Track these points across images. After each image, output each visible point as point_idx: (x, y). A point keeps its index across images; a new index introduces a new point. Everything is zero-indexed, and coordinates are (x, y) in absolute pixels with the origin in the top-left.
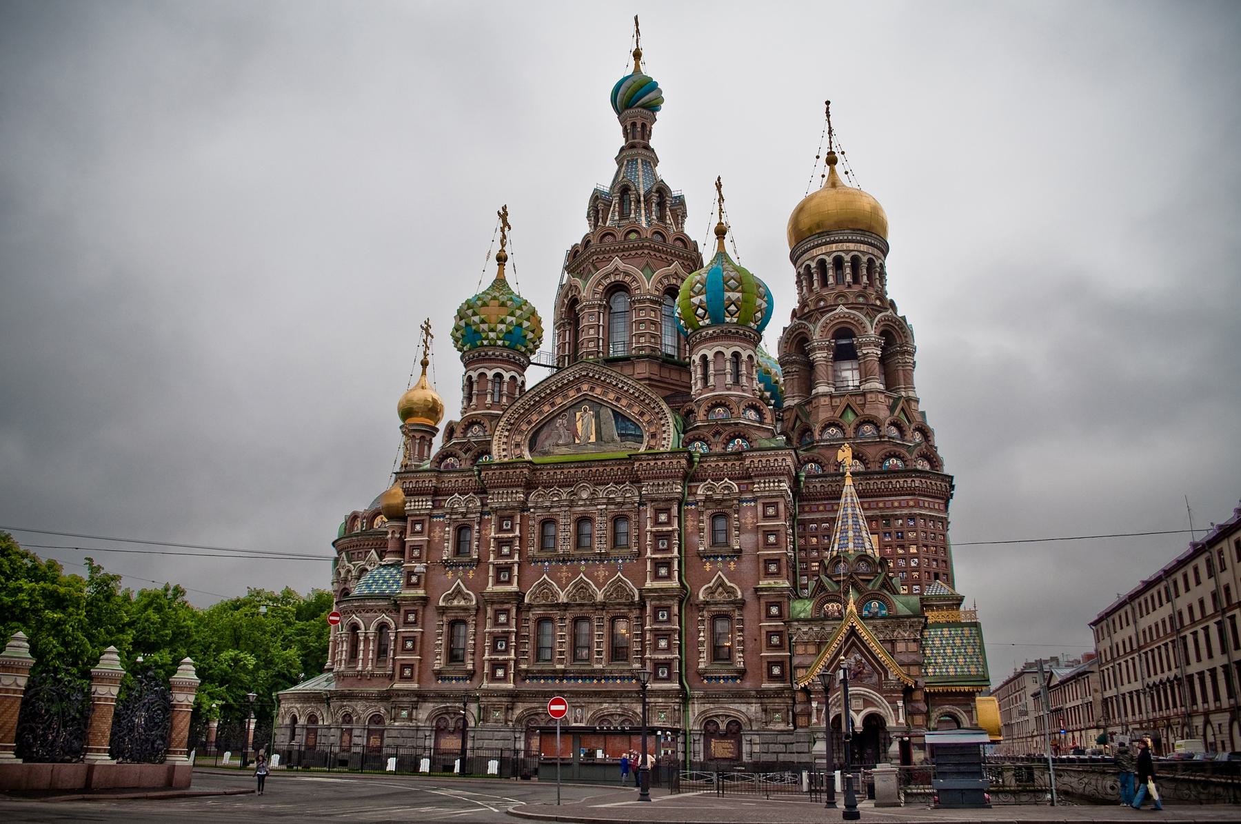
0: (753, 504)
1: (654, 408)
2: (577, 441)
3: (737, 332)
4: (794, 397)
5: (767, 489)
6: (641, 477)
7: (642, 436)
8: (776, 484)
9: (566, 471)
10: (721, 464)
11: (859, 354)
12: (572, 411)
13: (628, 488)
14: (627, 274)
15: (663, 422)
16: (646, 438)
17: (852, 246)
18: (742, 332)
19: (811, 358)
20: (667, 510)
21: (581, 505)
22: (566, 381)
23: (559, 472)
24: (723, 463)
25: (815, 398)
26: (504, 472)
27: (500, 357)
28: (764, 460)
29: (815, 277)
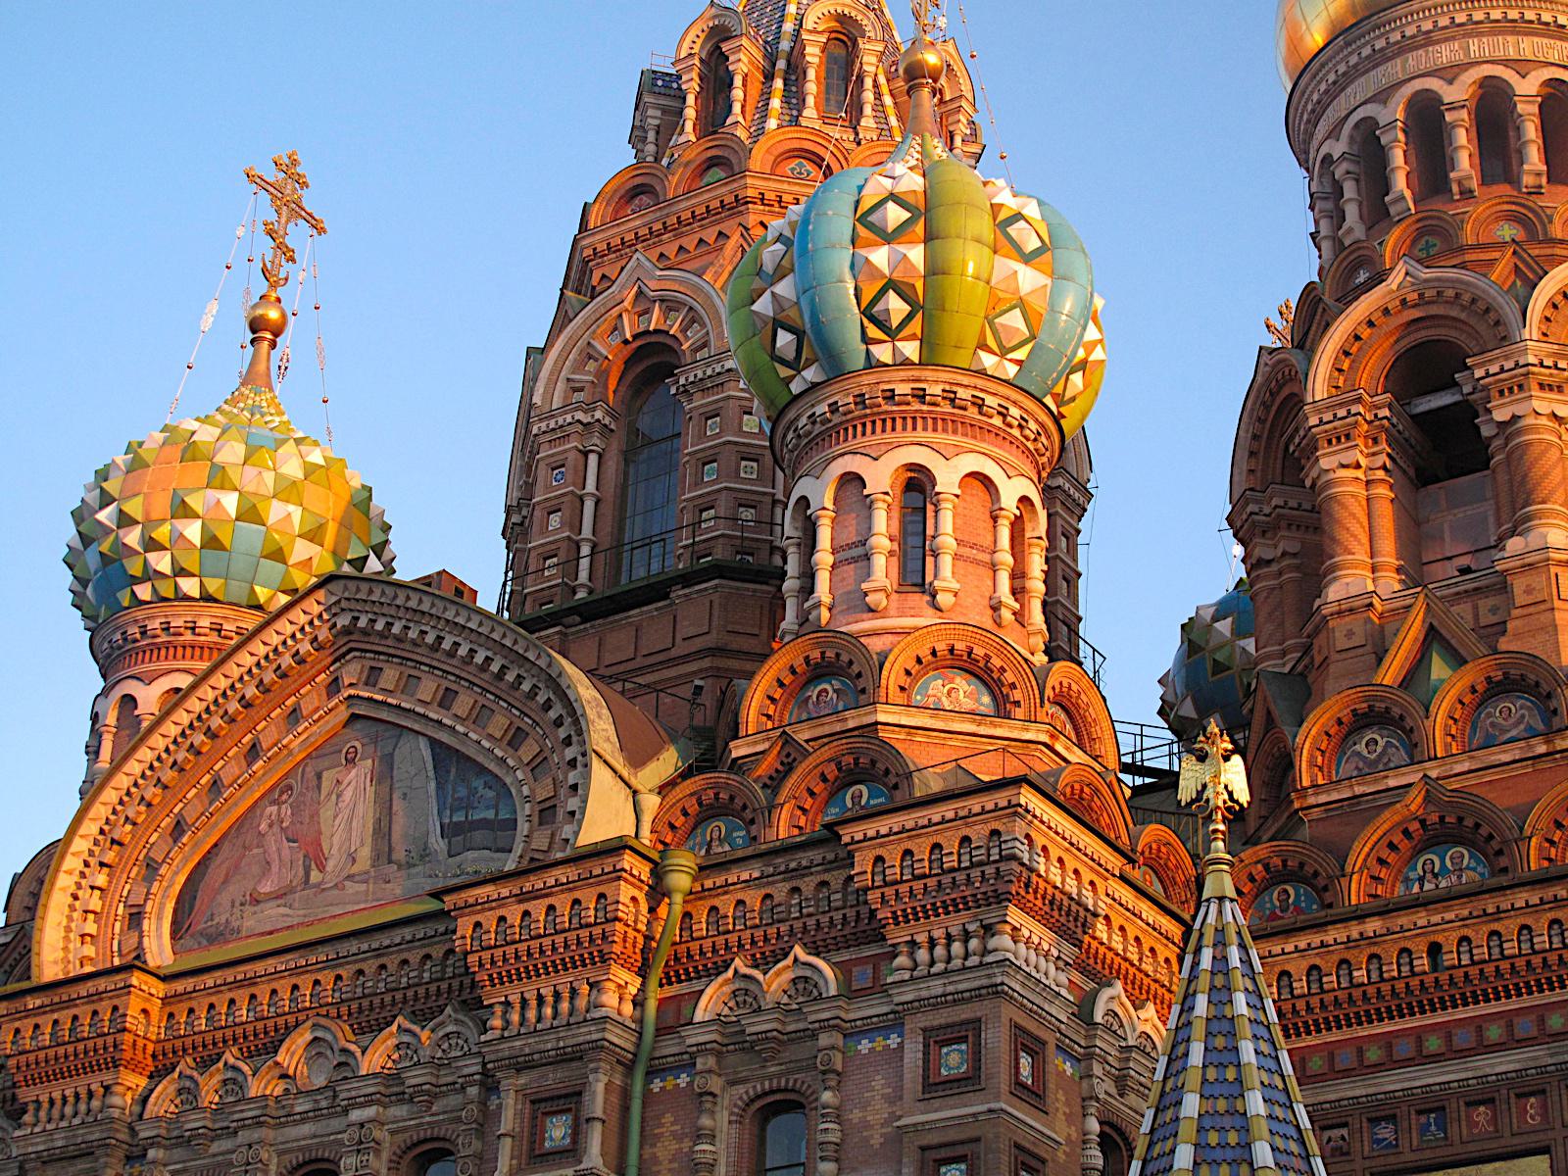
0: (894, 1041)
3: (920, 396)
4: (1284, 653)
5: (939, 967)
8: (974, 943)
10: (780, 892)
11: (1486, 431)
13: (451, 1028)
14: (670, 305)
15: (570, 753)
16: (523, 828)
17: (1476, 47)
18: (937, 390)
19: (1308, 483)
20: (570, 1100)
21: (304, 1118)
23: (242, 996)
24: (788, 886)
25: (1317, 631)
27: (188, 636)
28: (921, 848)
29: (1349, 189)
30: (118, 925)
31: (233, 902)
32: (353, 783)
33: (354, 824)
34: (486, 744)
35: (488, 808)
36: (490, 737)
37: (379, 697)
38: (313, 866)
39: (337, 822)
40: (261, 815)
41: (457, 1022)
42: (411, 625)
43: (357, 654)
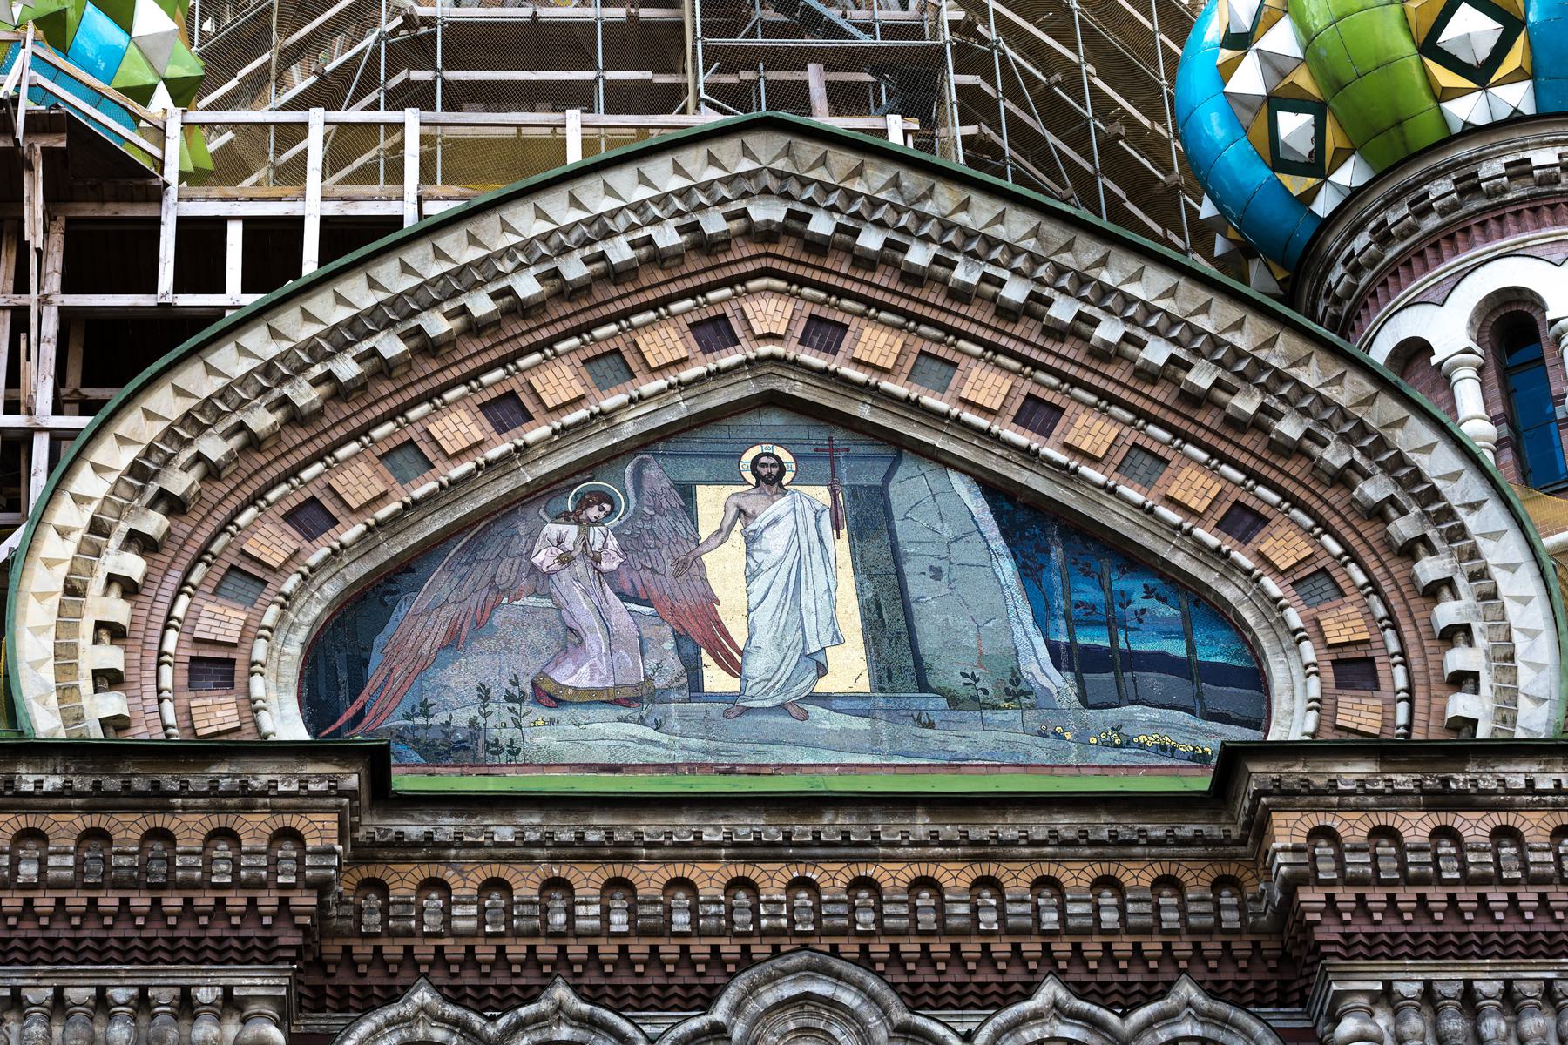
1: (1343, 478)
2: (716, 679)
6: (1328, 932)
7: (1257, 679)
9: (649, 878)
12: (656, 475)
15: (1429, 569)
22: (619, 251)
23: (587, 879)
26: (127, 828)
30: (167, 672)
31: (484, 694)
32: (786, 525)
33: (807, 599)
34: (1175, 517)
35: (1167, 635)
36: (1170, 501)
37: (859, 375)
38: (706, 658)
39: (759, 586)
40: (534, 536)
41: (1205, 1017)
42: (958, 258)
43: (781, 285)
